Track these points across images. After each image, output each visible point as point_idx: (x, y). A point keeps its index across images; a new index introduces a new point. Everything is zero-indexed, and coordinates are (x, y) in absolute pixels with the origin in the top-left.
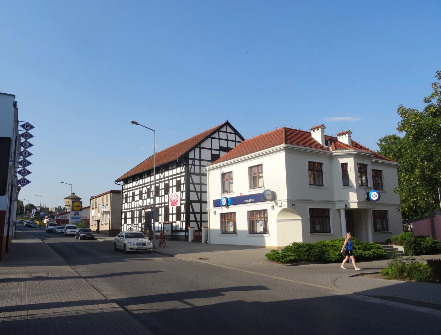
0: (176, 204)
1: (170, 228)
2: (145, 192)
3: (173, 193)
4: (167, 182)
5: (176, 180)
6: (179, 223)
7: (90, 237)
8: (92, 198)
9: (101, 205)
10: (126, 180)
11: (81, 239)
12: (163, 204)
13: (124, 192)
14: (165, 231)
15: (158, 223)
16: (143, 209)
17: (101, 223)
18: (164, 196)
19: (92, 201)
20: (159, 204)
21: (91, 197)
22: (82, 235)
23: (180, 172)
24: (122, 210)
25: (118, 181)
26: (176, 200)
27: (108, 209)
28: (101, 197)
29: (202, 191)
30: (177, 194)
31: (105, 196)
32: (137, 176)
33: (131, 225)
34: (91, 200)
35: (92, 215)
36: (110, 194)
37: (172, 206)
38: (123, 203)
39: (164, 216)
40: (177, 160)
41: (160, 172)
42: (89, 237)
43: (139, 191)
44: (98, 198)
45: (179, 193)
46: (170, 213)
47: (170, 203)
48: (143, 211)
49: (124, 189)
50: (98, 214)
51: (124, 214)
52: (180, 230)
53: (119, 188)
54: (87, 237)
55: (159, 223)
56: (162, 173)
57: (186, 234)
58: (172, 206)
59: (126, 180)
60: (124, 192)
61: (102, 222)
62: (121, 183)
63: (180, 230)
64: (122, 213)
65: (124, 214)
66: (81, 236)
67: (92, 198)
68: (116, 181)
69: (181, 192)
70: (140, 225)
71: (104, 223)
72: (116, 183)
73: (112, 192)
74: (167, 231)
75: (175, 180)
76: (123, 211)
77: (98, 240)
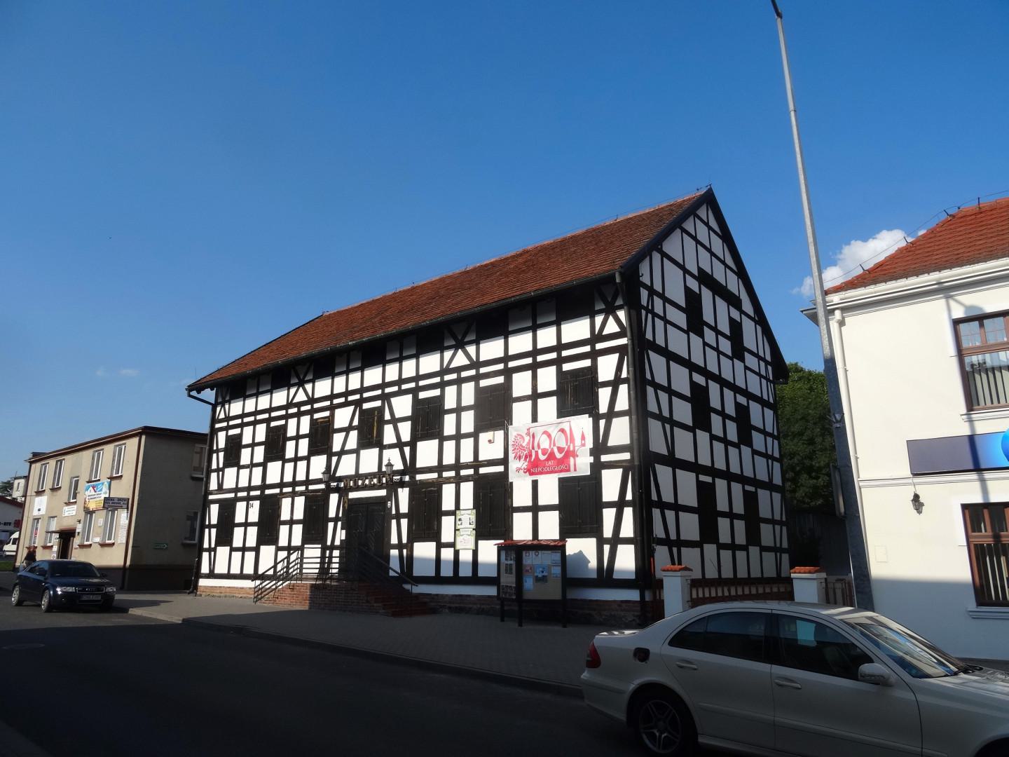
0: (563, 467)
1: (557, 571)
2: (346, 424)
3: (535, 419)
4: (237, 431)
5: (227, 434)
6: (582, 547)
7: (99, 598)
8: (38, 457)
9: (84, 478)
10: (232, 385)
11: (50, 609)
12: (288, 485)
13: (221, 429)
14: (529, 583)
15: (714, 546)
16: (337, 490)
17: (77, 541)
18: (356, 452)
19: (37, 467)
20: (281, 485)
21: (35, 454)
22: (59, 591)
23: (436, 368)
24: (208, 492)
25: (198, 387)
26: (560, 450)
27: (124, 489)
28: (88, 454)
29: (397, 450)
30: (562, 426)
31: (109, 449)
32: (301, 370)
33: (301, 549)
34: (31, 463)
35: (36, 513)
36: (136, 440)
37: (531, 474)
38: (214, 466)
39: (473, 518)
40: (613, 277)
41: (294, 380)
42: (92, 597)
43: (228, 437)
44: (67, 457)
45: (582, 424)
46: (444, 508)
47: (514, 465)
48: (334, 498)
49: (222, 416)
50: (66, 508)
51: (214, 509)
52: (594, 576)
53: (193, 418)
54: (85, 598)
55: (440, 546)
56: (301, 384)
57: (642, 596)
58: (534, 478)
59: (232, 385)
60: (221, 429)
61: (83, 538)
62: (209, 395)
63: (594, 576)
64: (206, 504)
65: (214, 509)
66: (55, 592)
67: (38, 457)
68: (190, 388)
69: (596, 417)
70: (313, 552)
71: (98, 540)
72: (194, 393)
73: (149, 432)
74: (542, 580)
75: (305, 420)
76: (211, 497)
77: (134, 611)
